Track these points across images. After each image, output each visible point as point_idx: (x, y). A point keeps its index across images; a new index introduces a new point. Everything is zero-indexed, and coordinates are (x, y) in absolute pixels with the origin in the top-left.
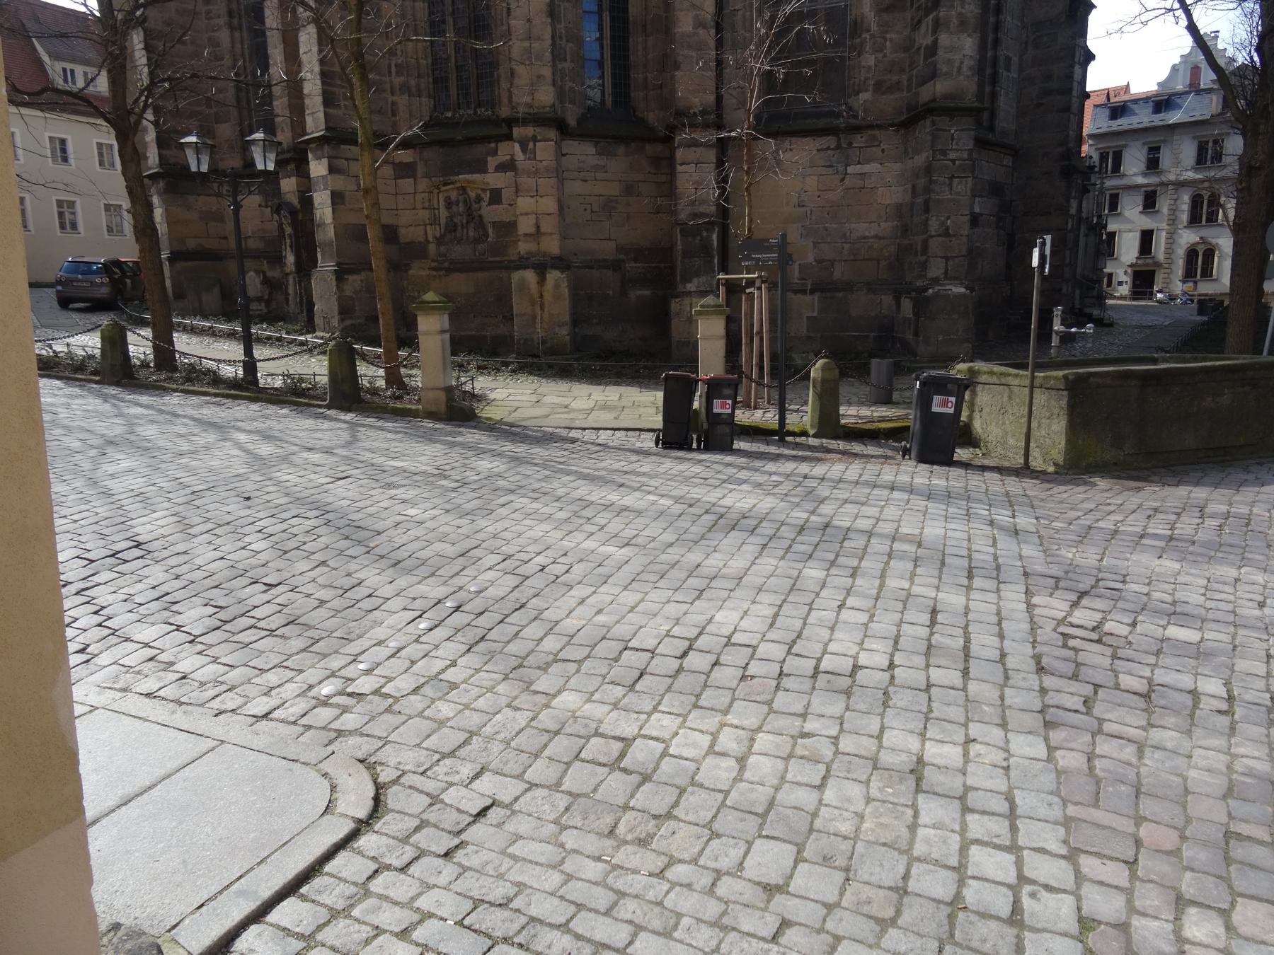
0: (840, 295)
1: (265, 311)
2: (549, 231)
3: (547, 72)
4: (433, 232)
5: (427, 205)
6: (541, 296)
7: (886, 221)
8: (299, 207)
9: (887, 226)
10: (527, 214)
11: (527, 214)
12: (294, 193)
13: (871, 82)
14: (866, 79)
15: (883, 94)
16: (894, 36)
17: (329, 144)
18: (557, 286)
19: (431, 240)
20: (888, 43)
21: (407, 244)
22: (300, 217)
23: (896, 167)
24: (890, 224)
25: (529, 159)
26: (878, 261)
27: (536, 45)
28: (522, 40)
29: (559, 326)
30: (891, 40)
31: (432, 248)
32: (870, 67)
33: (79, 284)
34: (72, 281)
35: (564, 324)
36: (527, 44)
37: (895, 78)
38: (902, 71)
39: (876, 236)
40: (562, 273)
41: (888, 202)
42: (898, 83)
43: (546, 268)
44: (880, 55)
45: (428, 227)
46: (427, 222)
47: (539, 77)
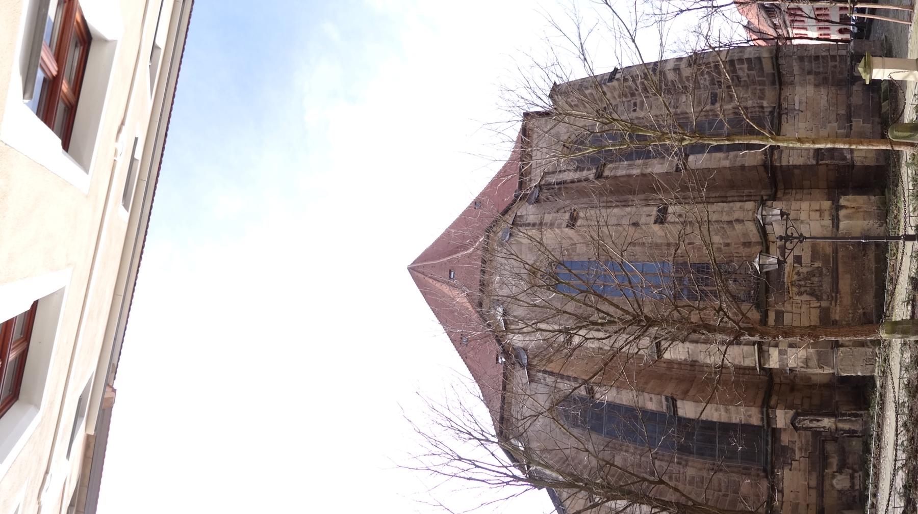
0: (852, 108)
1: (861, 473)
4: (815, 304)
7: (821, 92)
8: (794, 410)
9: (823, 91)
12: (786, 413)
13: (759, 101)
14: (757, 103)
15: (765, 96)
16: (742, 94)
20: (744, 96)
21: (820, 321)
23: (798, 88)
24: (822, 90)
26: (838, 94)
30: (743, 95)
31: (824, 304)
32: (753, 102)
37: (758, 91)
38: (755, 89)
39: (827, 96)
41: (813, 92)
42: (760, 90)
44: (749, 98)
45: (812, 306)
46: (808, 306)
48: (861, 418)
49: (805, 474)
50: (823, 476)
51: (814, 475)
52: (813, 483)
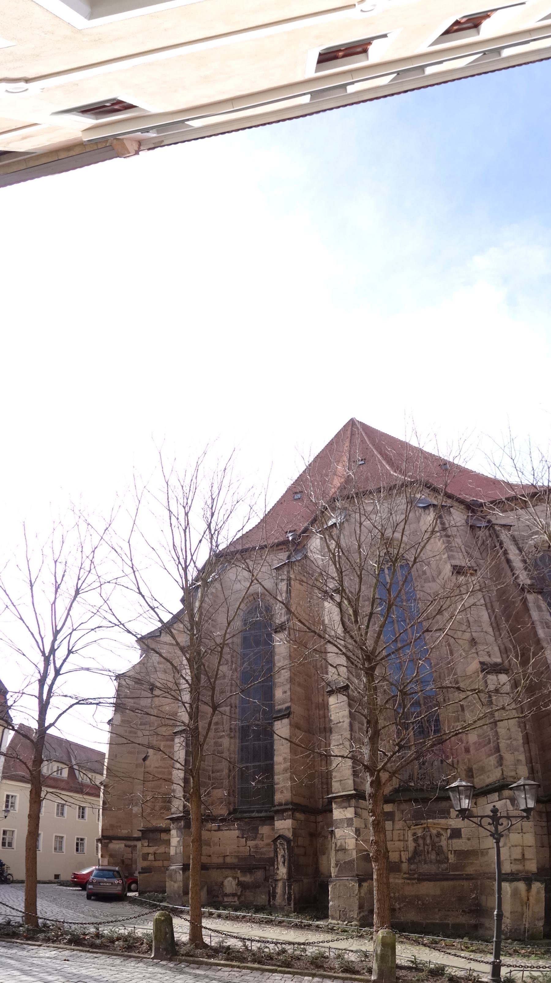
2: (530, 857)
3: (522, 757)
4: (405, 856)
5: (402, 838)
6: (528, 899)
10: (516, 846)
11: (516, 846)
17: (355, 798)
18: (538, 892)
19: (404, 861)
22: (292, 844)
25: (516, 810)
27: (514, 743)
28: (506, 740)
29: (538, 920)
33: (104, 884)
34: (100, 882)
35: (541, 919)
36: (509, 742)
40: (542, 884)
43: (532, 881)
47: (518, 760)
48: (286, 904)
49: (235, 852)
50: (234, 868)
51: (235, 861)
52: (229, 860)
